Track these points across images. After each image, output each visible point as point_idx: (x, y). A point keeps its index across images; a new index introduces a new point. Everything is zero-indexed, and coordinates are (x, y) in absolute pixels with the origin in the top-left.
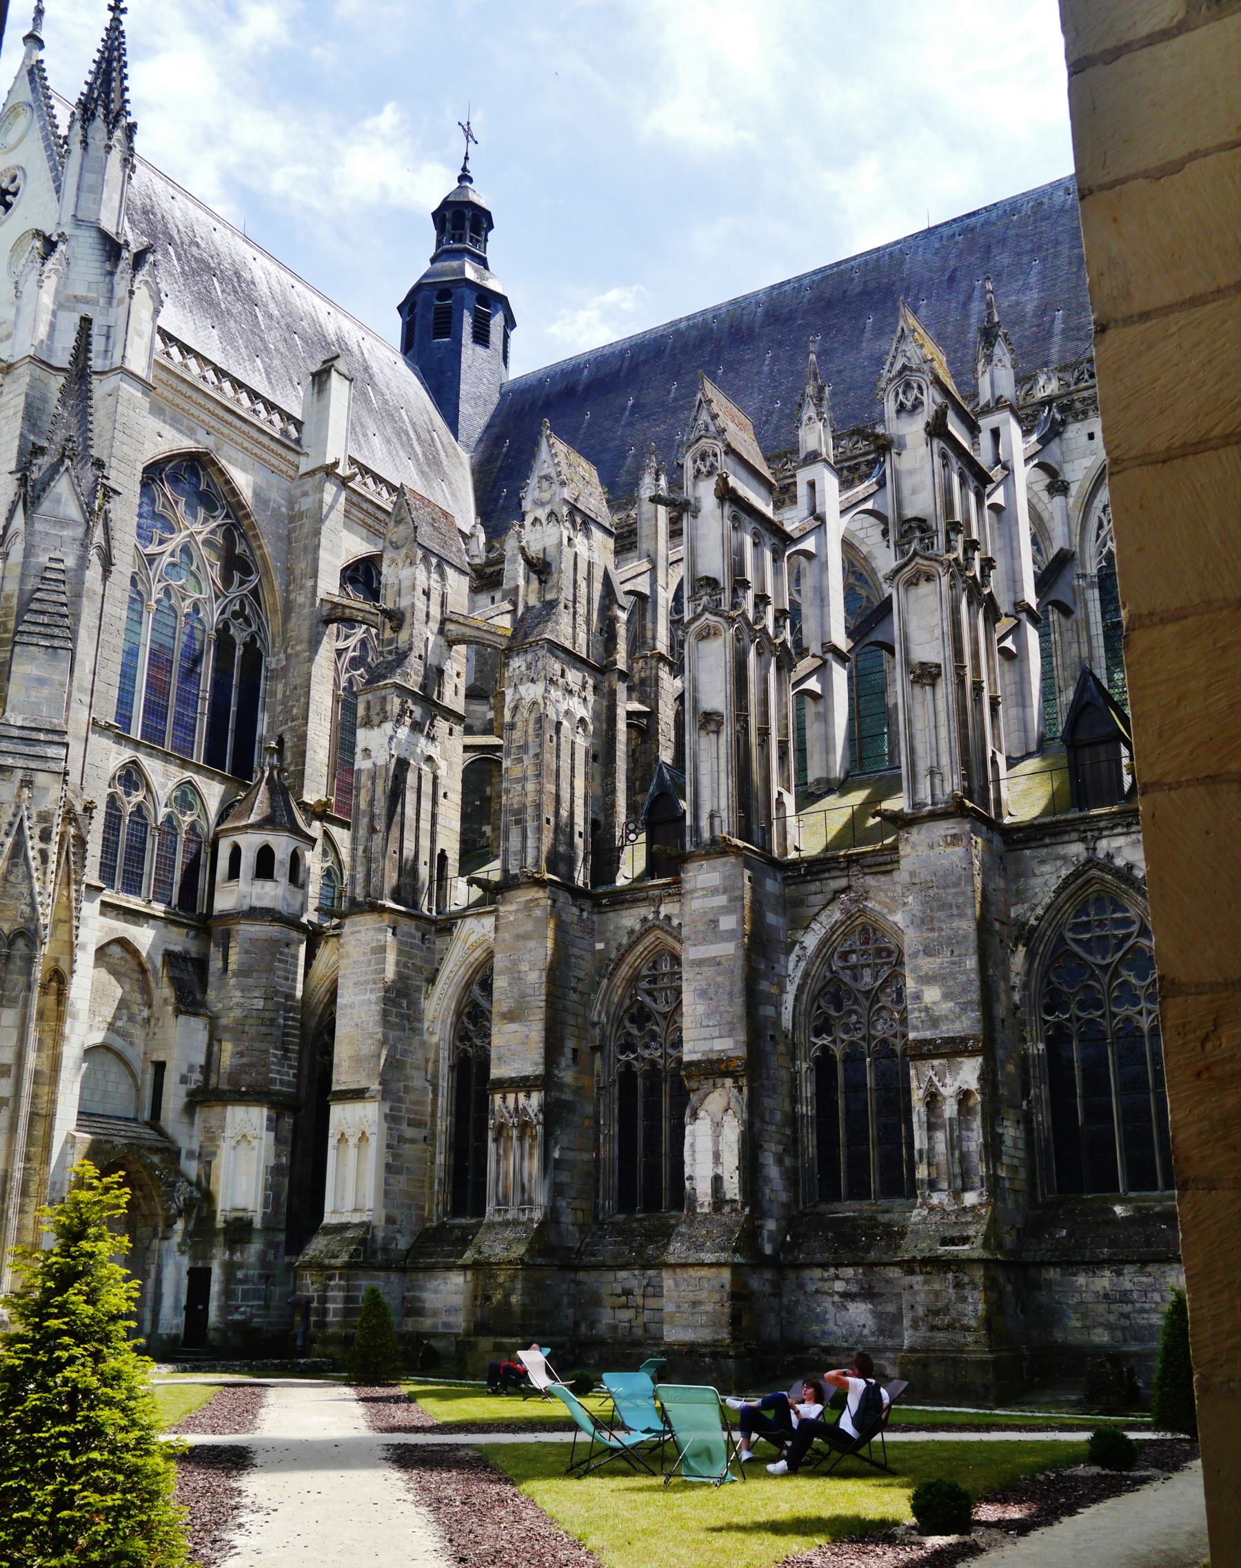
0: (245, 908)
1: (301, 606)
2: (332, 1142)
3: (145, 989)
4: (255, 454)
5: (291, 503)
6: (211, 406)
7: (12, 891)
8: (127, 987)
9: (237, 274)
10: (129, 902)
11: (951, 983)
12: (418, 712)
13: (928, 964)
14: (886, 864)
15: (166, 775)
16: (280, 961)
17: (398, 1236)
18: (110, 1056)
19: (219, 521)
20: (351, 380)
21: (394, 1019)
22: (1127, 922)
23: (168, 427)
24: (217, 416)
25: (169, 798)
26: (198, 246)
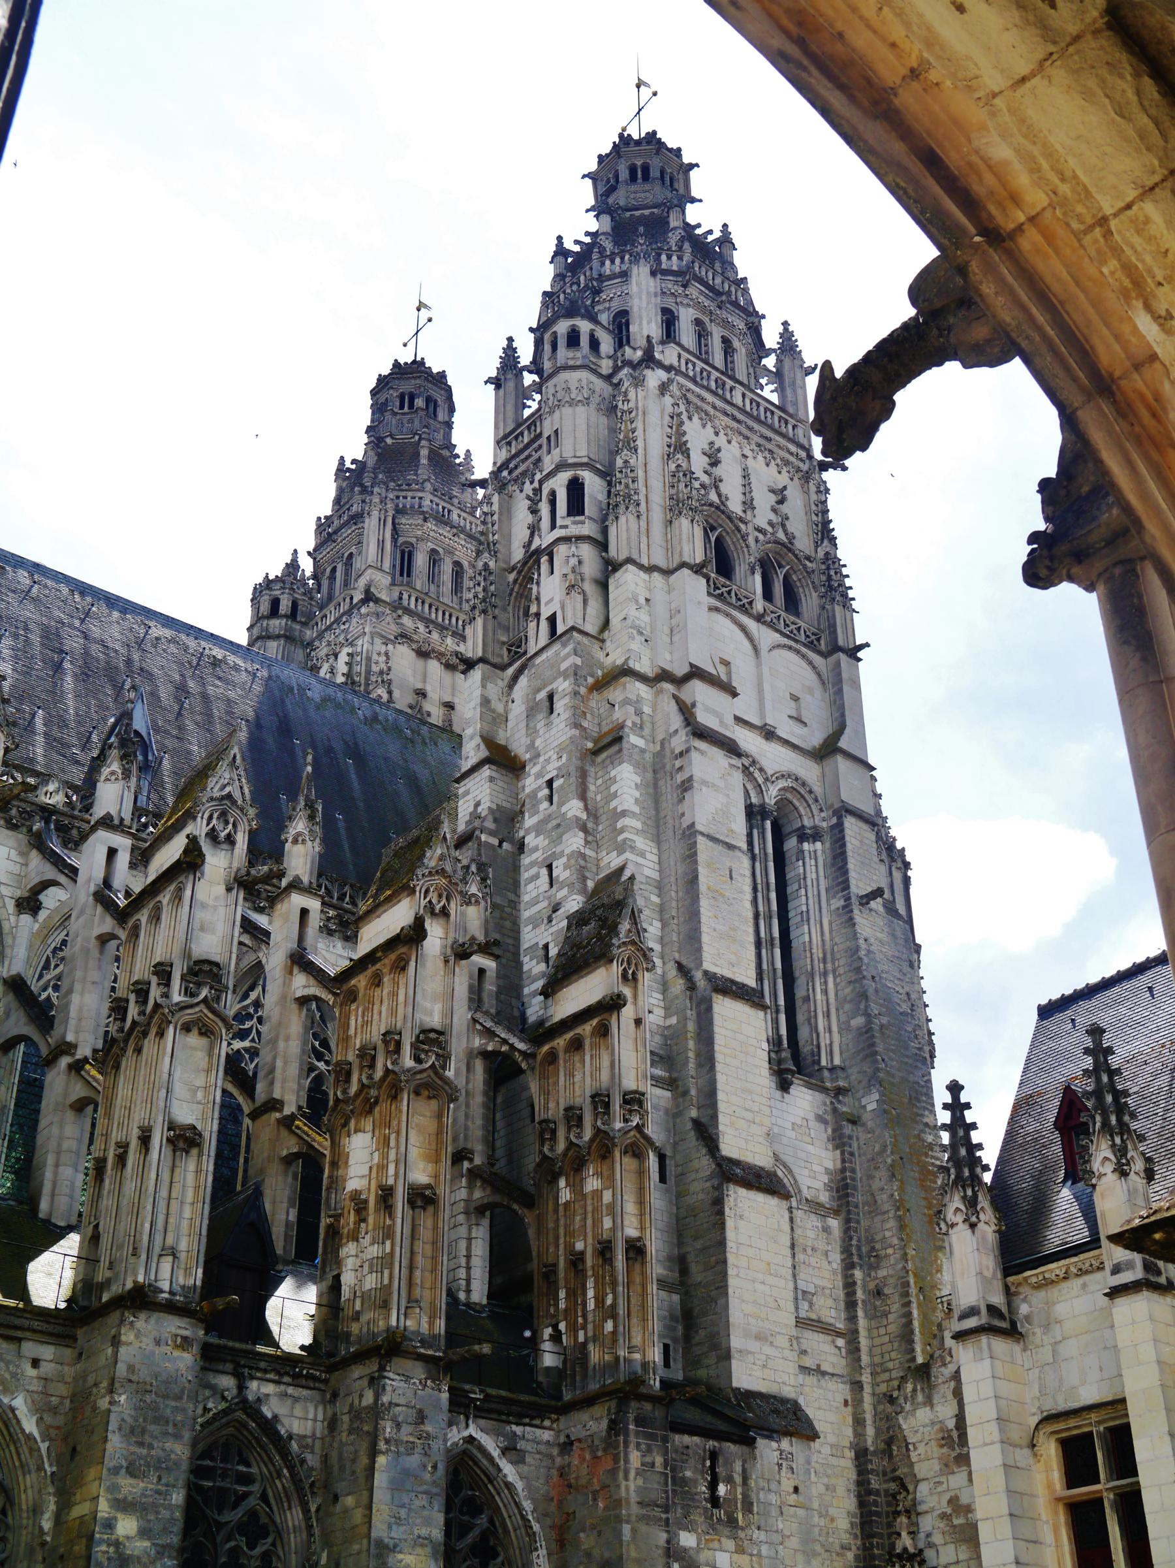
11: (151, 1517)
13: (129, 1486)
14: (16, 1328)
22: (246, 1479)
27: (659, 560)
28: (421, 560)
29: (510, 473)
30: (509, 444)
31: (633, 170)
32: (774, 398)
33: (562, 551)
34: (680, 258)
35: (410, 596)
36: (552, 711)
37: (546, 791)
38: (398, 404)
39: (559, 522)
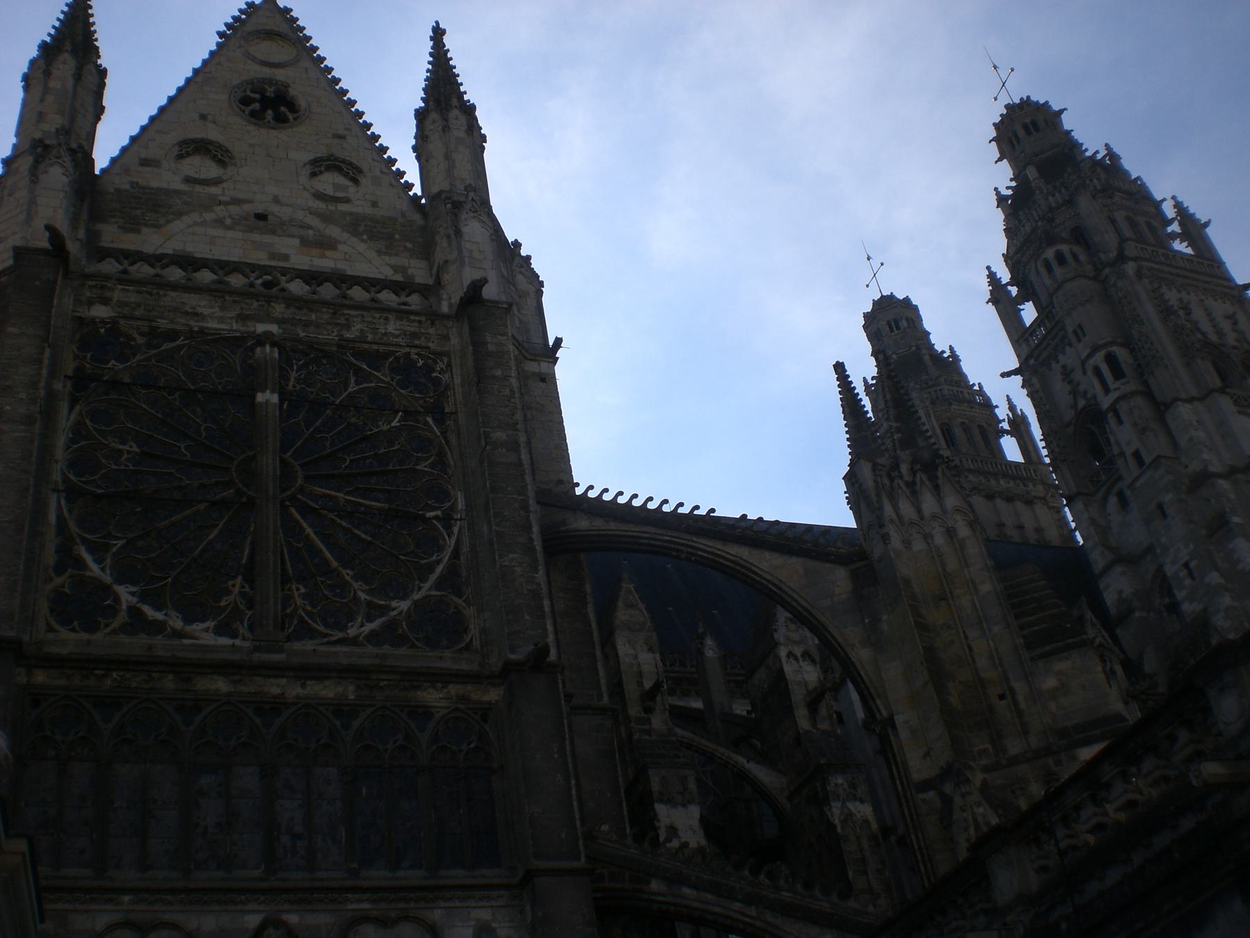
27: (1194, 392)
28: (958, 432)
29: (1036, 360)
30: (1027, 340)
31: (1025, 127)
32: (1189, 251)
33: (1123, 407)
34: (1099, 179)
35: (967, 460)
36: (1164, 515)
37: (1185, 572)
38: (888, 329)
39: (1112, 386)
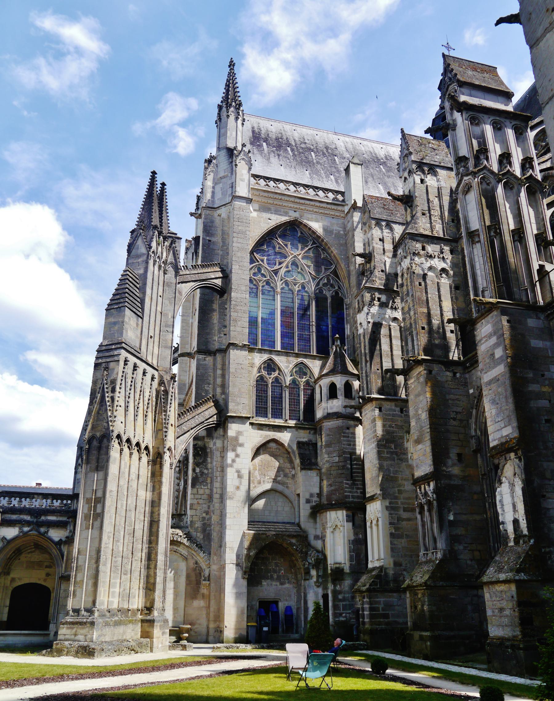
0: (325, 414)
1: (353, 271)
2: (368, 524)
3: (291, 462)
4: (321, 213)
5: (345, 228)
6: (292, 199)
7: (101, 417)
8: (282, 461)
9: (327, 148)
10: (275, 422)
12: (384, 298)
15: (288, 362)
16: (344, 437)
17: (405, 573)
18: (278, 494)
19: (309, 247)
20: (362, 165)
21: (385, 455)
23: (273, 215)
24: (296, 202)
25: (291, 371)
26: (305, 143)
